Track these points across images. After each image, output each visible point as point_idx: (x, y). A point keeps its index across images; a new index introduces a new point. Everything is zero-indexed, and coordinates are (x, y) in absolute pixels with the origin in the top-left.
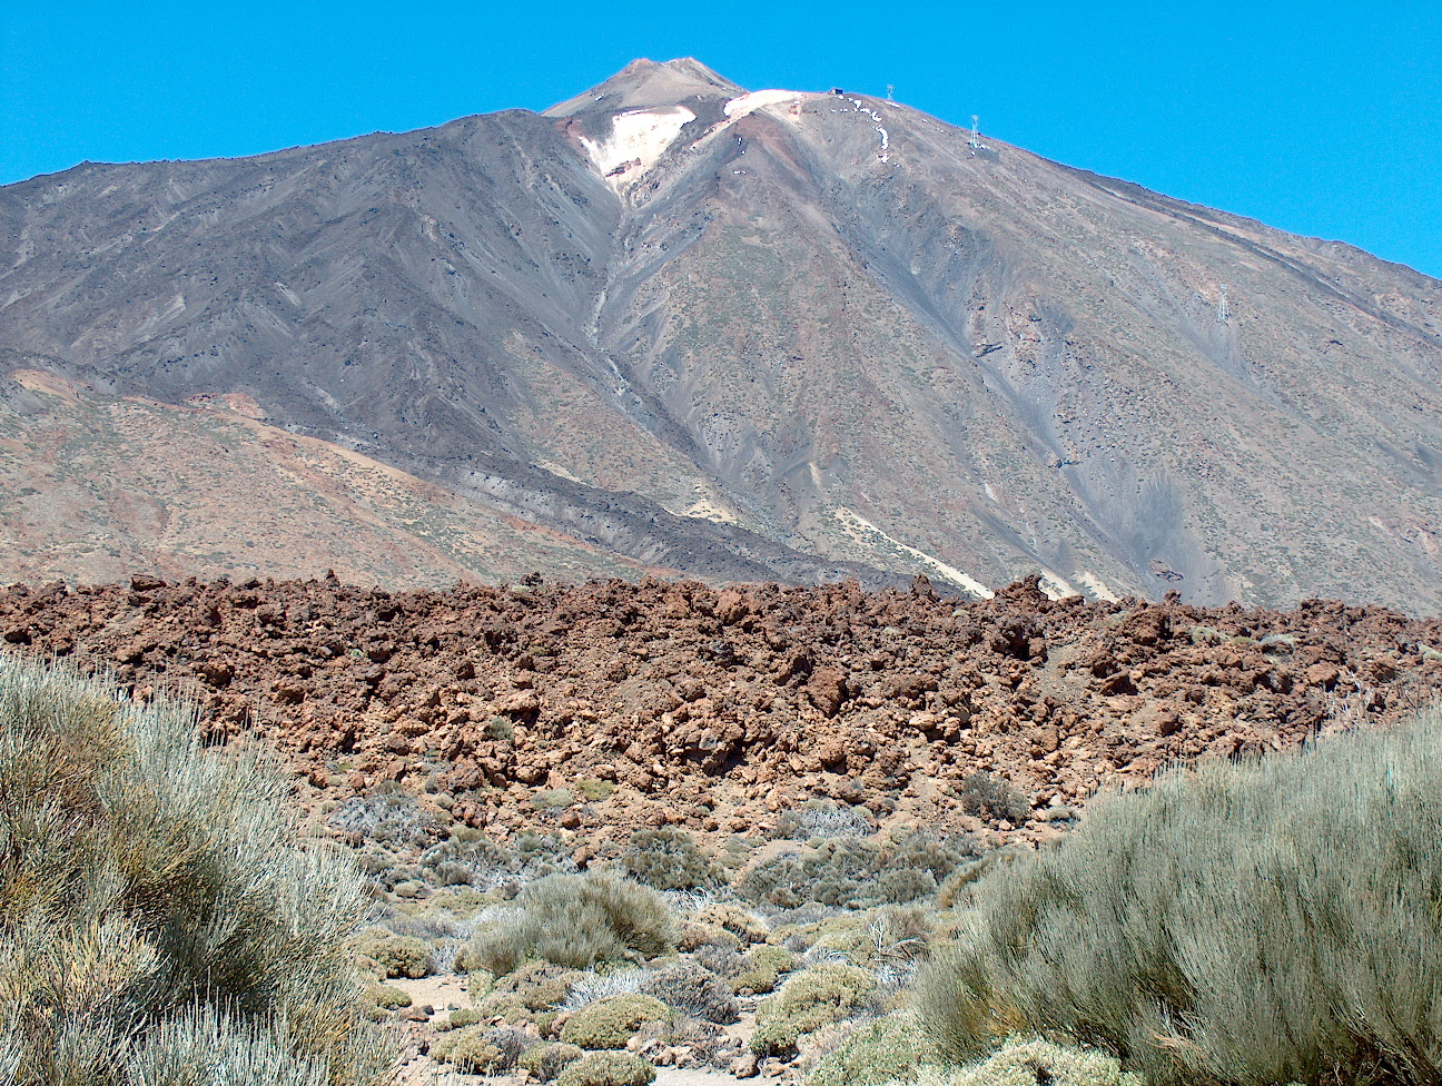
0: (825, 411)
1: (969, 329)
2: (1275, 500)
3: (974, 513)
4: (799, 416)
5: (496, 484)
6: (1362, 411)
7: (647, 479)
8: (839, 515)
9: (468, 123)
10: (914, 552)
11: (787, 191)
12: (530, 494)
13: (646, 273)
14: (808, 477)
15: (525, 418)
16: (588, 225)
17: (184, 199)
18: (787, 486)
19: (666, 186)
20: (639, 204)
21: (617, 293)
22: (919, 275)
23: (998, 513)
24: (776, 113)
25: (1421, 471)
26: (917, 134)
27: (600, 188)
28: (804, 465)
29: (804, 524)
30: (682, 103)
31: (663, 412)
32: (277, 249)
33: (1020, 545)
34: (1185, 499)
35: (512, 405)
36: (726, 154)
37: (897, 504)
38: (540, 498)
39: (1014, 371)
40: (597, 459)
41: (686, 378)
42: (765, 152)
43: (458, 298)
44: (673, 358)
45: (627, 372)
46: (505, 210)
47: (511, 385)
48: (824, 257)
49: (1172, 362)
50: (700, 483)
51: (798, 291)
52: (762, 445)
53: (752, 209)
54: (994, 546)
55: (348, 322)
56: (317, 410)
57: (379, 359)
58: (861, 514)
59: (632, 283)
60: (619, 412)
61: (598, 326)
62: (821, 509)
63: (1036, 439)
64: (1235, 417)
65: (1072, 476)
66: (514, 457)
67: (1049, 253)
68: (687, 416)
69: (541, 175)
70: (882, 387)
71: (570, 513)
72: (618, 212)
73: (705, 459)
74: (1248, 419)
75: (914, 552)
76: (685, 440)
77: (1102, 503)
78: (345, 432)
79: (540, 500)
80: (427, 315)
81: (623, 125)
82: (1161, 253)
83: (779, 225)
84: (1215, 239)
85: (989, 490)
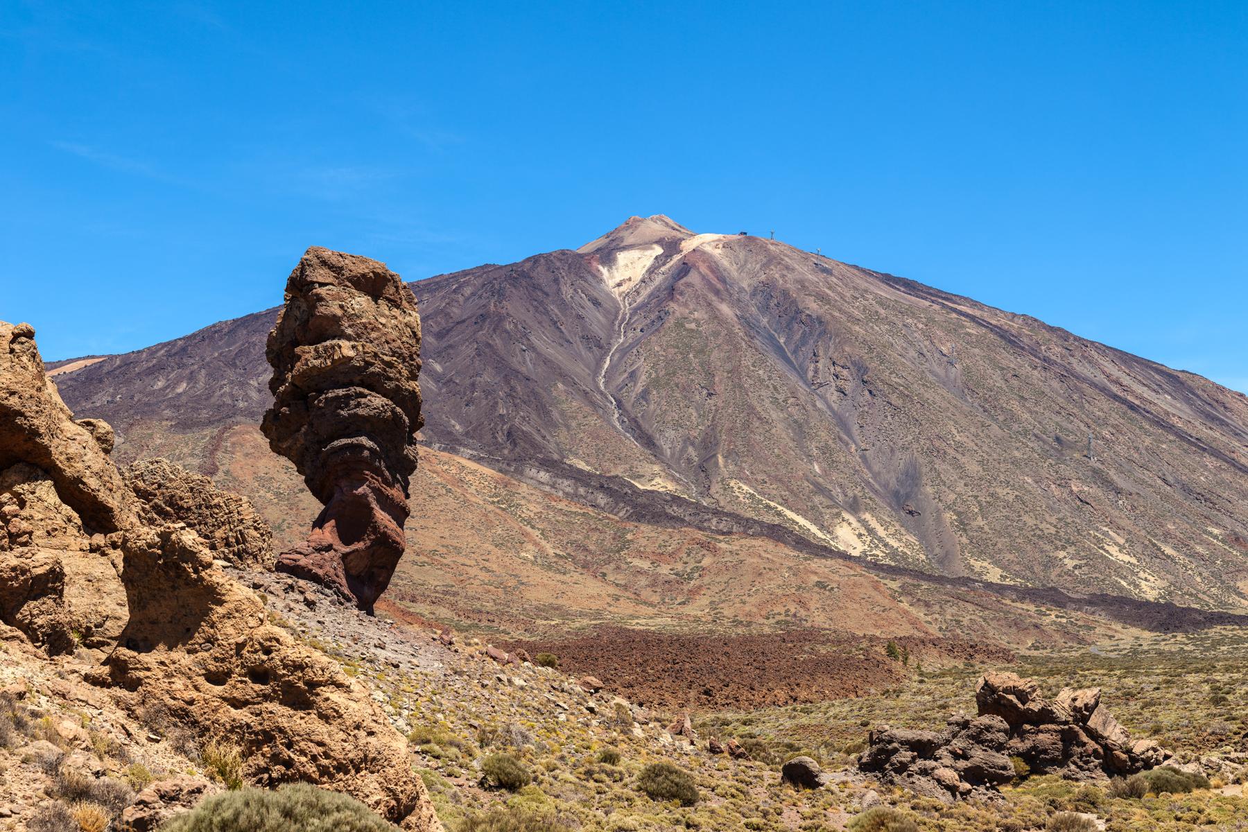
0: (728, 425)
2: (973, 468)
4: (713, 427)
7: (627, 466)
8: (732, 484)
10: (772, 504)
13: (631, 346)
14: (717, 463)
15: (563, 436)
18: (704, 470)
21: (615, 358)
23: (821, 480)
25: (1056, 450)
28: (715, 455)
29: (713, 491)
31: (639, 427)
33: (831, 498)
34: (924, 470)
35: (556, 426)
37: (765, 477)
41: (652, 407)
43: (526, 364)
44: (645, 395)
45: (620, 405)
47: (555, 414)
48: (730, 334)
49: (922, 391)
50: (656, 468)
51: (715, 355)
52: (693, 444)
54: (817, 499)
56: (450, 433)
57: (484, 402)
59: (624, 351)
60: (614, 427)
62: (723, 480)
63: (845, 437)
64: (956, 422)
65: (863, 457)
66: (556, 457)
68: (651, 428)
70: (759, 409)
73: (662, 454)
74: (963, 422)
76: (649, 442)
77: (879, 473)
78: (465, 446)
80: (509, 374)
83: (706, 317)
85: (816, 467)
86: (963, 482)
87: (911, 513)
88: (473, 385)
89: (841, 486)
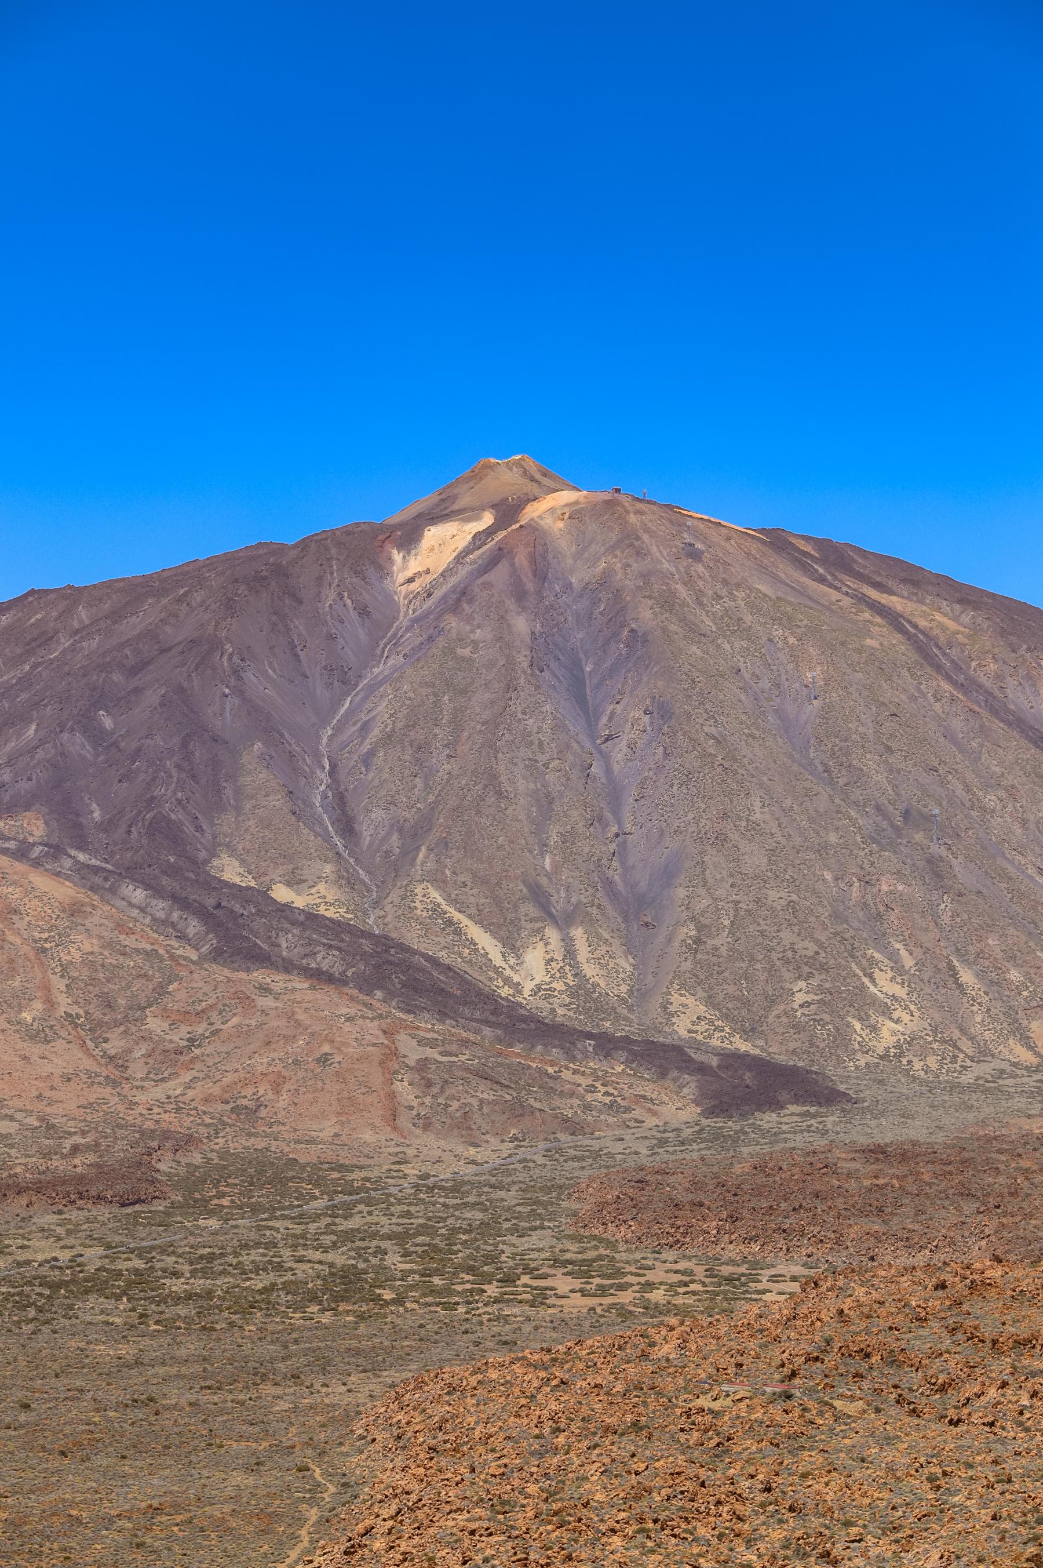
0: (453, 802)
1: (604, 720)
3: (524, 882)
5: (139, 895)
6: (879, 777)
9: (304, 544)
10: (457, 916)
11: (511, 604)
12: (155, 902)
14: (415, 858)
15: (226, 822)
16: (362, 635)
17: (87, 622)
18: (396, 868)
19: (438, 594)
20: (414, 611)
21: (358, 699)
22: (590, 672)
23: (544, 881)
24: (548, 522)
26: (645, 537)
27: (389, 599)
28: (418, 849)
30: (493, 506)
32: (117, 677)
36: (488, 564)
38: (161, 904)
39: (620, 756)
40: (263, 853)
41: (371, 775)
42: (513, 564)
44: (367, 760)
45: (332, 773)
46: (299, 625)
47: (229, 792)
50: (328, 869)
52: (401, 831)
53: (475, 623)
55: (134, 745)
58: (438, 888)
61: (333, 728)
67: (694, 648)
69: (339, 594)
71: (175, 915)
72: (395, 618)
73: (357, 844)
75: (457, 916)
79: (160, 907)
81: (432, 534)
82: (792, 640)
84: (867, 615)
86: (731, 881)
87: (647, 924)
88: (139, 750)
89: (568, 888)
